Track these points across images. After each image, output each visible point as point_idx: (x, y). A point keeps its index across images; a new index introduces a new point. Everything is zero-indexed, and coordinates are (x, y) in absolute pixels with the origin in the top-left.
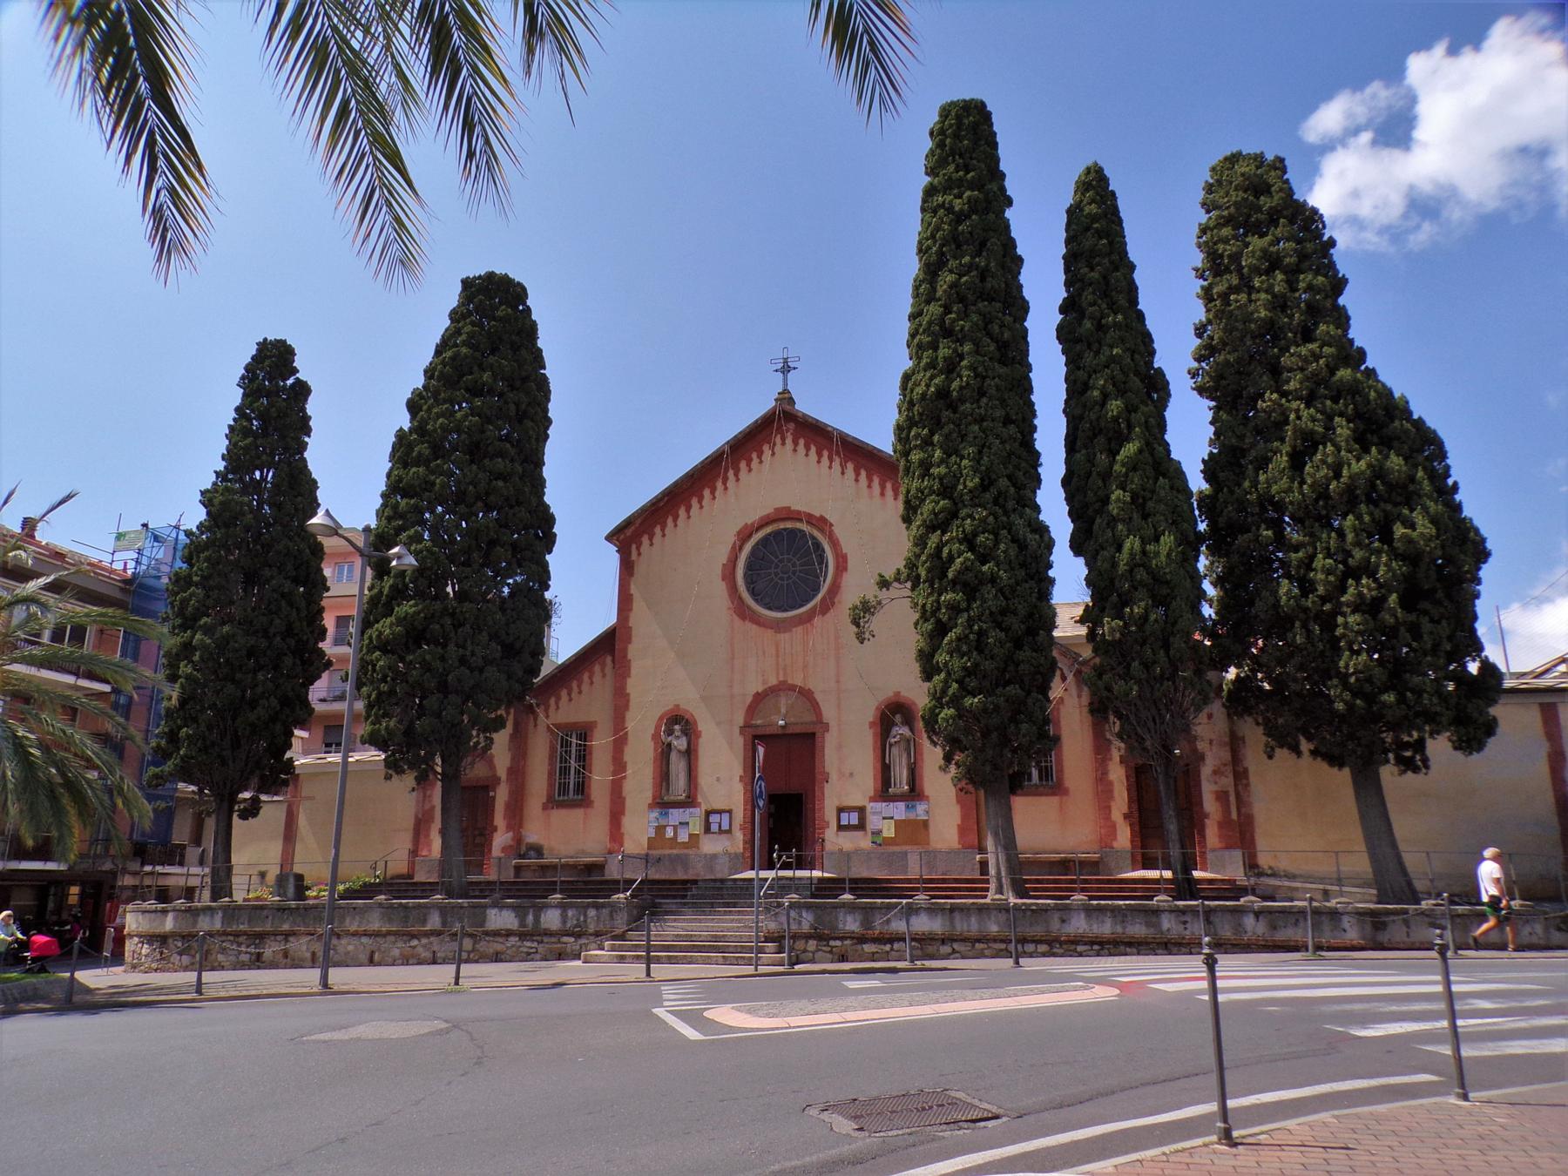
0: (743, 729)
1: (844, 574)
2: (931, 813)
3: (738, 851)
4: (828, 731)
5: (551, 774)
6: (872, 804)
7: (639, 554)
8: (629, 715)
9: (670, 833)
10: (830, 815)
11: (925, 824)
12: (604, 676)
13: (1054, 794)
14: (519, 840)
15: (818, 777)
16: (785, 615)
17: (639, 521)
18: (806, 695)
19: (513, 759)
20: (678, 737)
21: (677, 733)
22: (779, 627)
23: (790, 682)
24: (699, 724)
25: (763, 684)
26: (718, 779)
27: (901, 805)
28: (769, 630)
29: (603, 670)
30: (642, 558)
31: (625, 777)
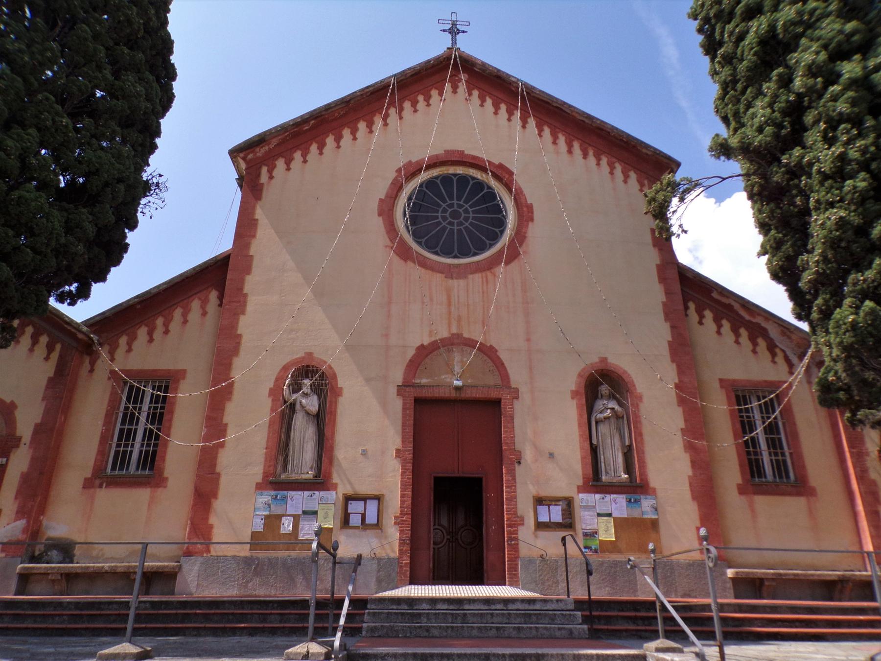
0: (401, 390)
1: (530, 224)
2: (659, 509)
3: (392, 555)
4: (517, 398)
5: (105, 439)
6: (581, 496)
7: (271, 177)
8: (237, 362)
9: (287, 525)
10: (525, 507)
11: (654, 524)
12: (204, 314)
13: (799, 494)
14: (34, 532)
15: (507, 456)
16: (456, 261)
17: (275, 142)
18: (489, 352)
19: (47, 412)
20: (306, 395)
21: (306, 389)
22: (449, 272)
23: (466, 335)
24: (339, 379)
25: (430, 336)
26: (364, 453)
27: (622, 499)
28: (439, 275)
29: (203, 307)
30: (273, 181)
31: (222, 445)
